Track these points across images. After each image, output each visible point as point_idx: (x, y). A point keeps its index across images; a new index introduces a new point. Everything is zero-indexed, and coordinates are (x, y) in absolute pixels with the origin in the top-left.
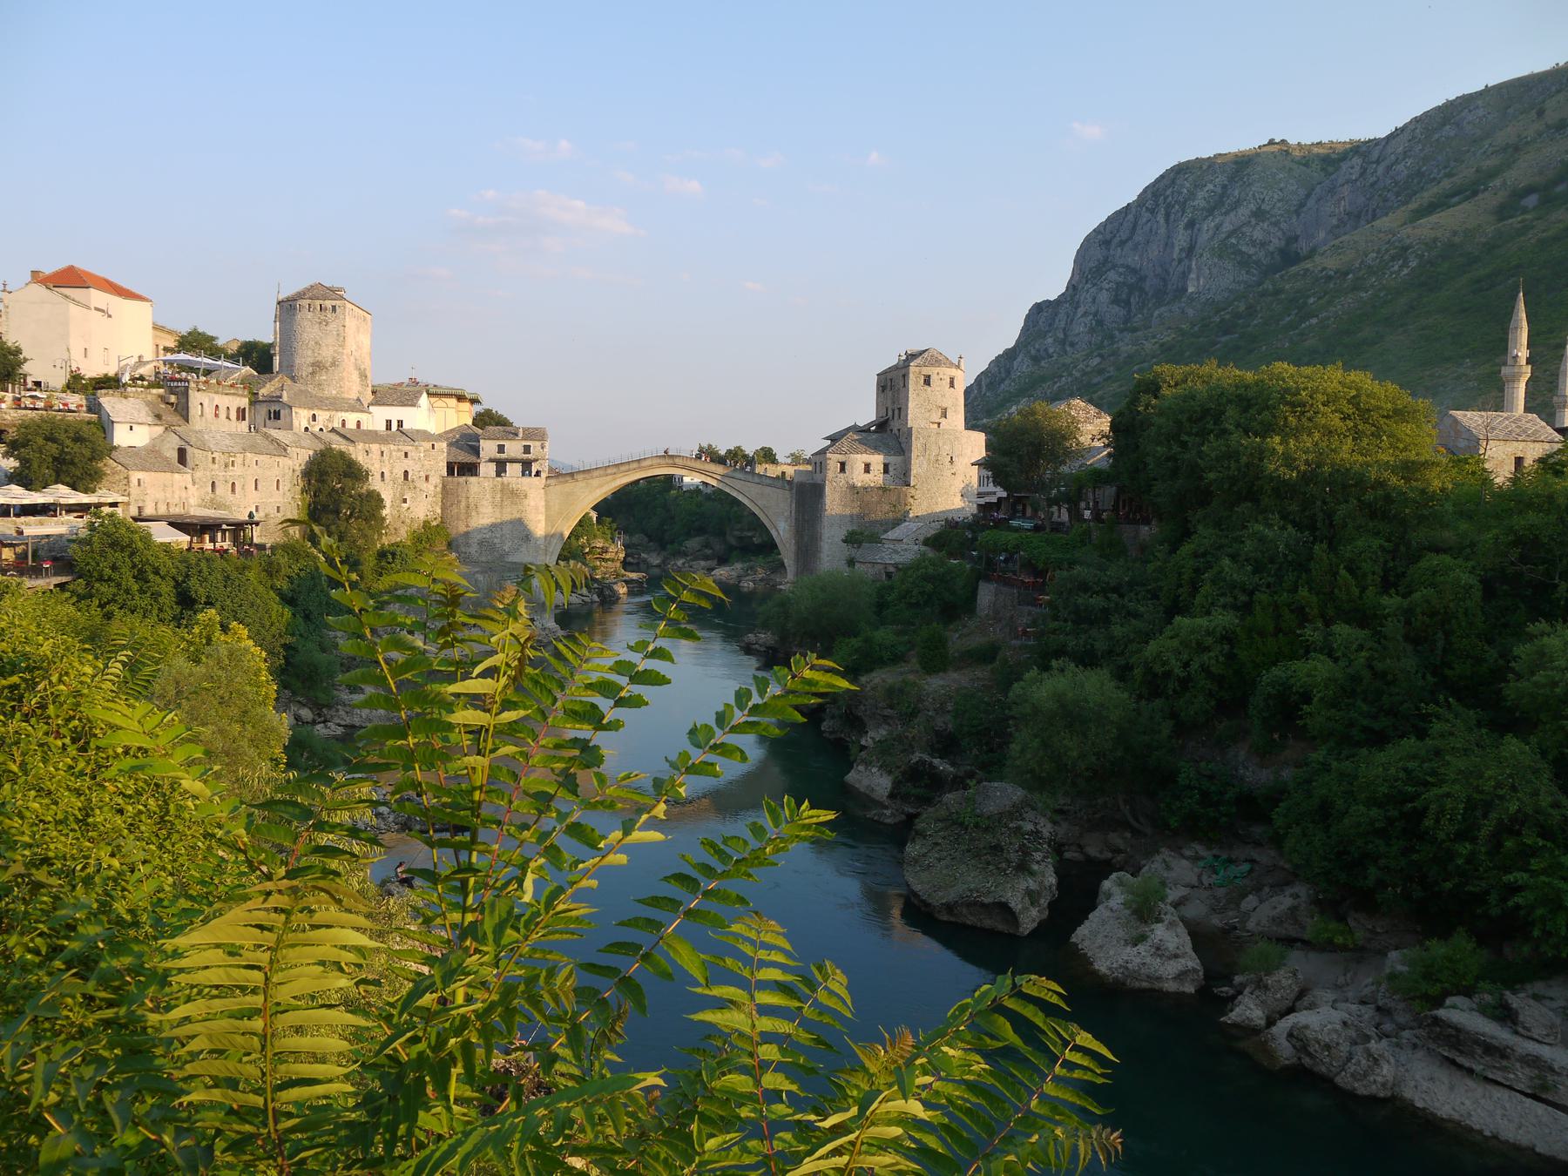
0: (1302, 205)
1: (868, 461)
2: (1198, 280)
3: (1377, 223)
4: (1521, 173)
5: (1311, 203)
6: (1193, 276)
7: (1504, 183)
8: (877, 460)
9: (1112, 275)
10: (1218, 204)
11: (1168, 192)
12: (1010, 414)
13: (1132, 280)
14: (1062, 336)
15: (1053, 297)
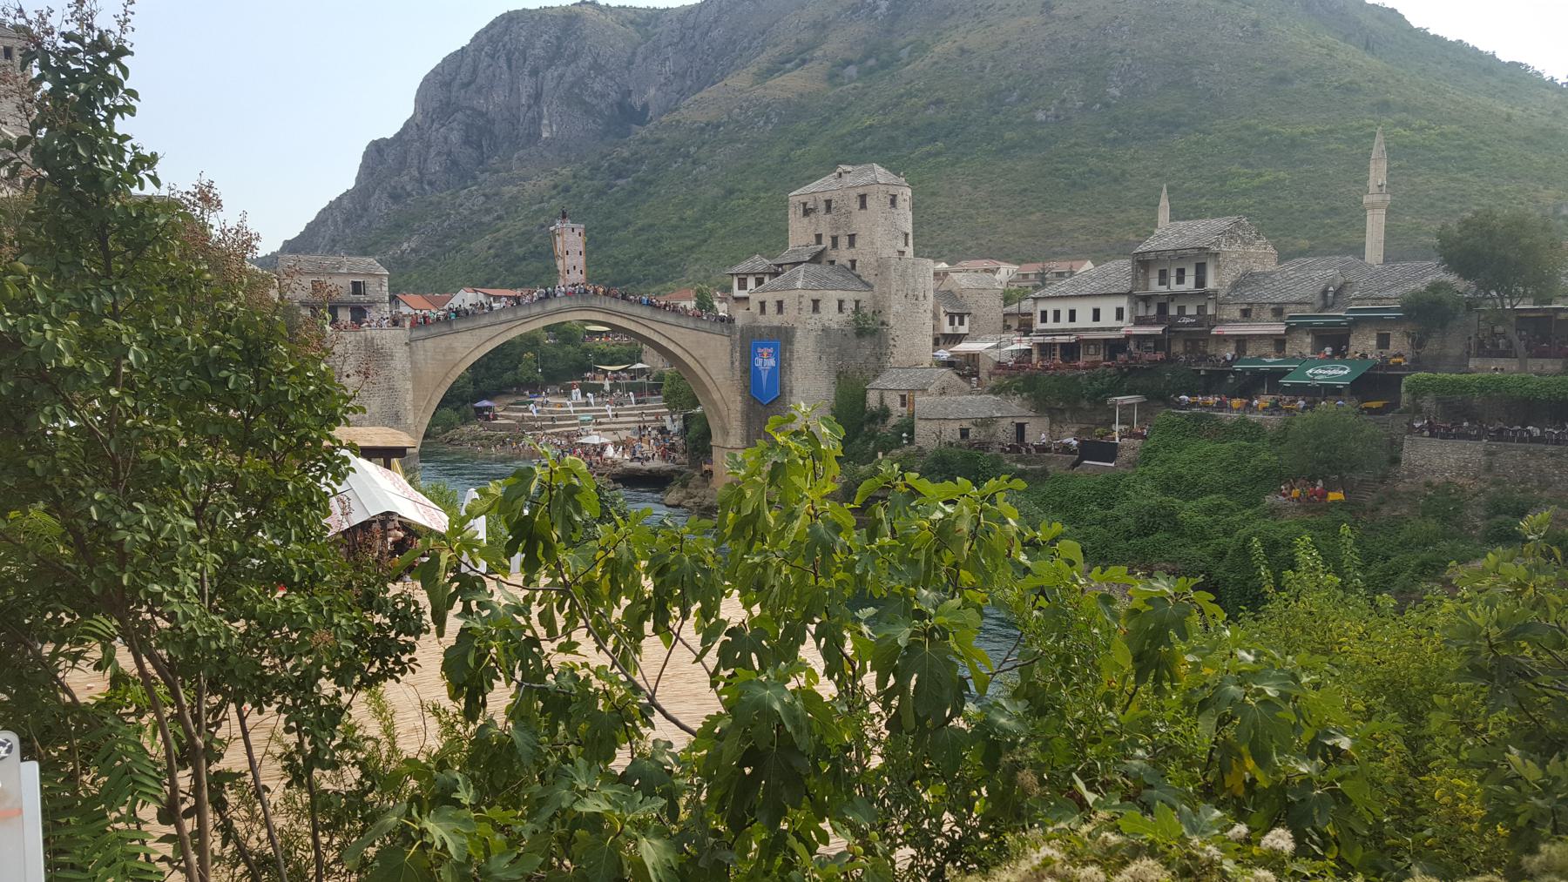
0: (631, 63)
1: (842, 297)
2: (551, 126)
3: (729, 81)
4: (835, 45)
5: (639, 59)
6: (545, 122)
7: (825, 55)
8: (849, 297)
9: (459, 115)
10: (555, 55)
11: (506, 38)
12: (403, 252)
13: (481, 122)
14: (416, 174)
15: (389, 135)
